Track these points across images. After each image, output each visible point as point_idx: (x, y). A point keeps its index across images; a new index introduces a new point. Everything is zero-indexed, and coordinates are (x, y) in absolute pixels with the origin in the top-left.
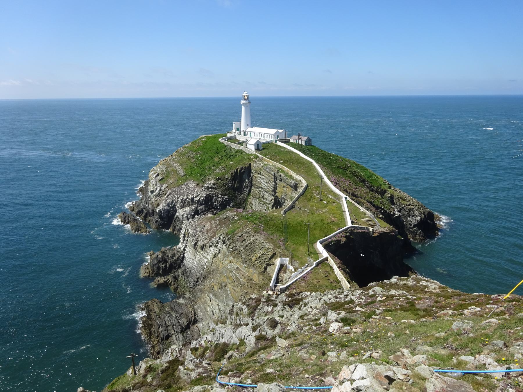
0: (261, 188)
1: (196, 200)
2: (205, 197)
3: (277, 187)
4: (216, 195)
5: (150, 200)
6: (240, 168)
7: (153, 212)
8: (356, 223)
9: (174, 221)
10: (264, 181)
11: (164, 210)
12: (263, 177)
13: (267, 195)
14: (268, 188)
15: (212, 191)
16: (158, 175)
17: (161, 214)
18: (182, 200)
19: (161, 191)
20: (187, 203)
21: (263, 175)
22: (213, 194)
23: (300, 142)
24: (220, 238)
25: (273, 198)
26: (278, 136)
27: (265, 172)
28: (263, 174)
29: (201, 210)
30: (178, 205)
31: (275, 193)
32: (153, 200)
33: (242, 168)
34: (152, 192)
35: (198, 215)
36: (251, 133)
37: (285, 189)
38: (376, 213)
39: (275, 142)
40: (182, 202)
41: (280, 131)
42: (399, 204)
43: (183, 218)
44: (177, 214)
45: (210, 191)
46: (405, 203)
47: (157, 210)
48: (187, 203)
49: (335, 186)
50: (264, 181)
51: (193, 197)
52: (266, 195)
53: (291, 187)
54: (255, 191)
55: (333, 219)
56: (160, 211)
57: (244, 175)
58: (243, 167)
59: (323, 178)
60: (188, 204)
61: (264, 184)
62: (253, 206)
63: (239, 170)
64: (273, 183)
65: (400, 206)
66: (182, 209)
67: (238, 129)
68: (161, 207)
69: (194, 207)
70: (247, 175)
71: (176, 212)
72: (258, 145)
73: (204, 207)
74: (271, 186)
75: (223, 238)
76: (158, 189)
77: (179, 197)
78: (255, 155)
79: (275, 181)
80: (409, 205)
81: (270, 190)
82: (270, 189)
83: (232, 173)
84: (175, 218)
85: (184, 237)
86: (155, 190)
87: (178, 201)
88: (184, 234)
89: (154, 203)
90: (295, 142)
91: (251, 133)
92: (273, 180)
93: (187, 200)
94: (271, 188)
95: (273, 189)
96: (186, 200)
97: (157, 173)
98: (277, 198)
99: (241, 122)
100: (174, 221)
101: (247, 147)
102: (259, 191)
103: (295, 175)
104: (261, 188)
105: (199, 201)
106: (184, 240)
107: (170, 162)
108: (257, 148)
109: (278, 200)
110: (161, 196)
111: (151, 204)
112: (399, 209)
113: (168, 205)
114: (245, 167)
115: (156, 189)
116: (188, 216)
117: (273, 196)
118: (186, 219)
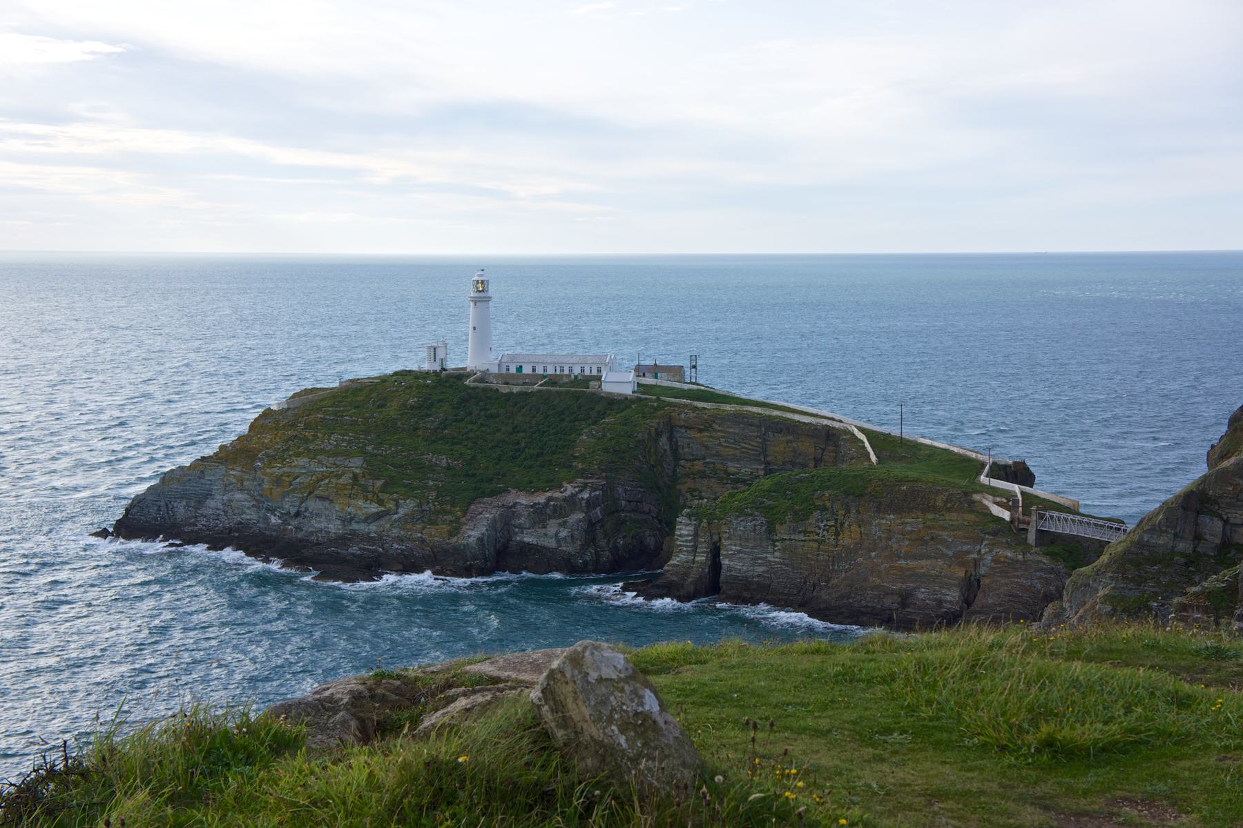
1: (583, 499)
10: (725, 442)
14: (742, 452)
16: (355, 477)
17: (484, 545)
37: (795, 445)
43: (558, 541)
52: (732, 467)
56: (480, 540)
60: (555, 511)
69: (581, 516)
96: (546, 504)
98: (768, 463)
102: (708, 463)
105: (588, 500)
113: (493, 523)
117: (761, 464)
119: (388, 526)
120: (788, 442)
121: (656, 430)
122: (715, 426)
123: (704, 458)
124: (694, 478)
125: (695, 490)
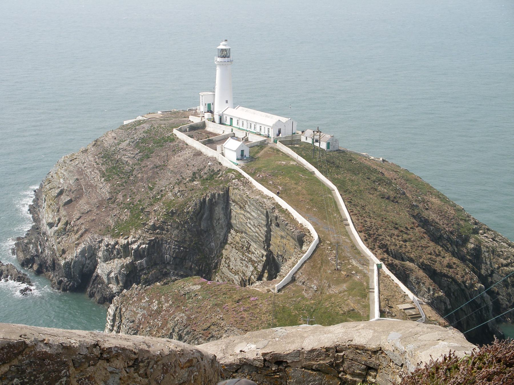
0: (246, 233)
1: (132, 249)
2: (148, 244)
3: (272, 236)
4: (167, 242)
5: (47, 240)
6: (209, 195)
7: (54, 265)
8: (388, 312)
9: (91, 283)
10: (250, 223)
11: (75, 263)
12: (249, 215)
13: (255, 246)
15: (160, 234)
16: (61, 193)
17: (70, 268)
18: (107, 246)
19: (68, 226)
20: (115, 252)
21: (248, 212)
22: (162, 240)
23: (317, 144)
24: (174, 331)
25: (265, 253)
26: (279, 132)
27: (253, 207)
28: (249, 210)
29: (140, 267)
30: (100, 254)
31: (269, 245)
32: (53, 241)
33: (213, 196)
34: (51, 225)
35: (137, 284)
36: (231, 119)
37: (285, 241)
38: (431, 288)
39: (275, 142)
40: (107, 250)
41: (284, 120)
42: (489, 263)
43: (109, 279)
44: (99, 271)
45: (157, 234)
46: (502, 260)
47: (62, 263)
48: (115, 252)
49: (365, 241)
50: (250, 223)
51: (128, 242)
52: (254, 246)
53: (293, 239)
54: (233, 236)
55: (352, 305)
56: (68, 265)
57: (217, 208)
58: (214, 194)
59: (348, 225)
60: (118, 253)
61: (250, 228)
62: (231, 263)
63: (207, 199)
64: (266, 229)
65: (491, 266)
66: (107, 262)
67: (209, 105)
68: (70, 257)
69: (128, 260)
70: (223, 208)
71: (95, 267)
72: (242, 151)
73: (146, 261)
74: (262, 233)
75: (180, 330)
76: (63, 220)
77: (102, 240)
78: (237, 172)
79: (268, 225)
80: (507, 265)
81: (260, 240)
82: (260, 238)
83: (196, 204)
84: (94, 278)
85: (114, 320)
86: (57, 222)
87: (99, 247)
88: (114, 316)
89: (55, 247)
90: (311, 143)
91: (231, 119)
92: (264, 223)
93: (117, 247)
94: (261, 237)
95: (265, 239)
96: (114, 246)
97: (59, 190)
99: (214, 92)
100: (91, 283)
101: (223, 154)
103: (300, 219)
104: (246, 233)
105: (137, 250)
106: (113, 326)
107: (83, 167)
108: (240, 157)
109: (273, 258)
110: (68, 235)
111: (50, 249)
112: (489, 272)
113: (83, 252)
114: (219, 195)
115: (59, 220)
116: (117, 276)
117: (265, 250)
118: (114, 281)
119: (53, 233)
120: (282, 237)
121: (211, 200)
122: (247, 206)
123: (242, 232)
124: (233, 247)
125: (228, 258)
